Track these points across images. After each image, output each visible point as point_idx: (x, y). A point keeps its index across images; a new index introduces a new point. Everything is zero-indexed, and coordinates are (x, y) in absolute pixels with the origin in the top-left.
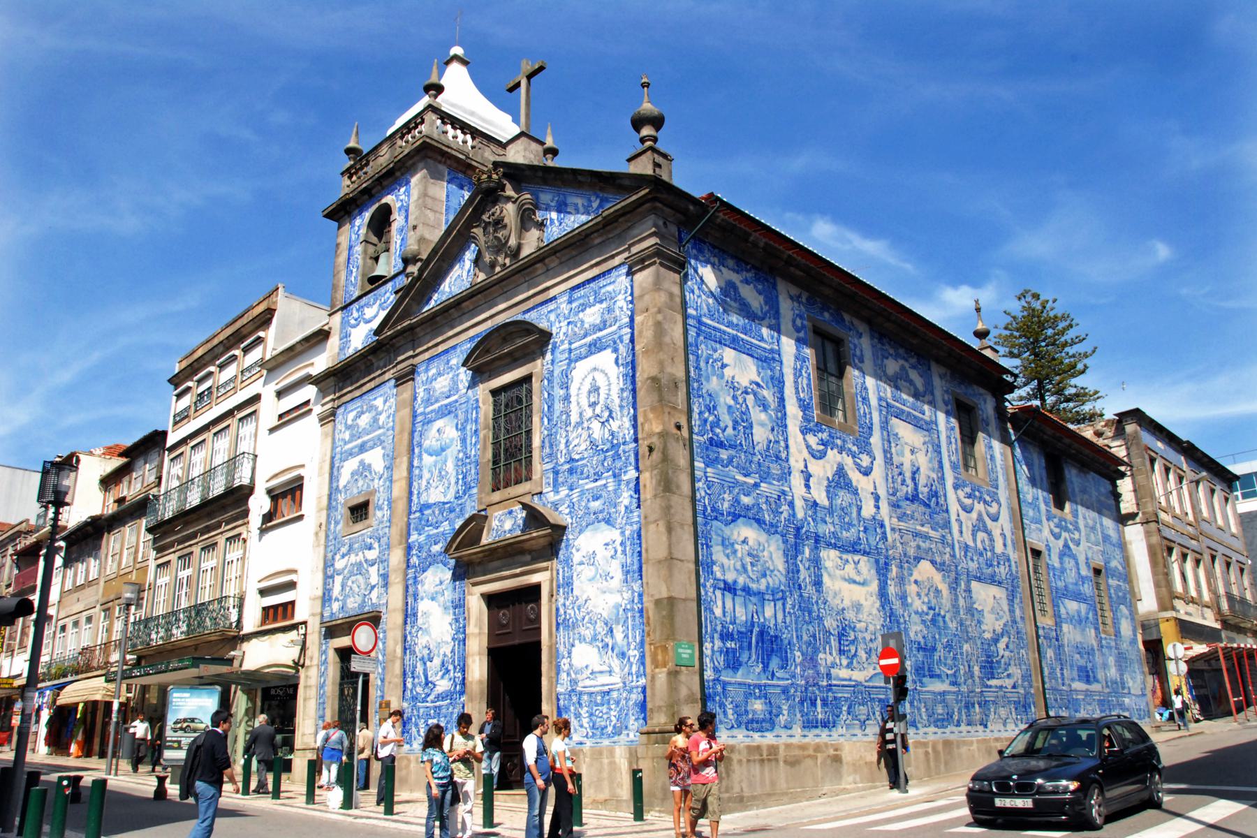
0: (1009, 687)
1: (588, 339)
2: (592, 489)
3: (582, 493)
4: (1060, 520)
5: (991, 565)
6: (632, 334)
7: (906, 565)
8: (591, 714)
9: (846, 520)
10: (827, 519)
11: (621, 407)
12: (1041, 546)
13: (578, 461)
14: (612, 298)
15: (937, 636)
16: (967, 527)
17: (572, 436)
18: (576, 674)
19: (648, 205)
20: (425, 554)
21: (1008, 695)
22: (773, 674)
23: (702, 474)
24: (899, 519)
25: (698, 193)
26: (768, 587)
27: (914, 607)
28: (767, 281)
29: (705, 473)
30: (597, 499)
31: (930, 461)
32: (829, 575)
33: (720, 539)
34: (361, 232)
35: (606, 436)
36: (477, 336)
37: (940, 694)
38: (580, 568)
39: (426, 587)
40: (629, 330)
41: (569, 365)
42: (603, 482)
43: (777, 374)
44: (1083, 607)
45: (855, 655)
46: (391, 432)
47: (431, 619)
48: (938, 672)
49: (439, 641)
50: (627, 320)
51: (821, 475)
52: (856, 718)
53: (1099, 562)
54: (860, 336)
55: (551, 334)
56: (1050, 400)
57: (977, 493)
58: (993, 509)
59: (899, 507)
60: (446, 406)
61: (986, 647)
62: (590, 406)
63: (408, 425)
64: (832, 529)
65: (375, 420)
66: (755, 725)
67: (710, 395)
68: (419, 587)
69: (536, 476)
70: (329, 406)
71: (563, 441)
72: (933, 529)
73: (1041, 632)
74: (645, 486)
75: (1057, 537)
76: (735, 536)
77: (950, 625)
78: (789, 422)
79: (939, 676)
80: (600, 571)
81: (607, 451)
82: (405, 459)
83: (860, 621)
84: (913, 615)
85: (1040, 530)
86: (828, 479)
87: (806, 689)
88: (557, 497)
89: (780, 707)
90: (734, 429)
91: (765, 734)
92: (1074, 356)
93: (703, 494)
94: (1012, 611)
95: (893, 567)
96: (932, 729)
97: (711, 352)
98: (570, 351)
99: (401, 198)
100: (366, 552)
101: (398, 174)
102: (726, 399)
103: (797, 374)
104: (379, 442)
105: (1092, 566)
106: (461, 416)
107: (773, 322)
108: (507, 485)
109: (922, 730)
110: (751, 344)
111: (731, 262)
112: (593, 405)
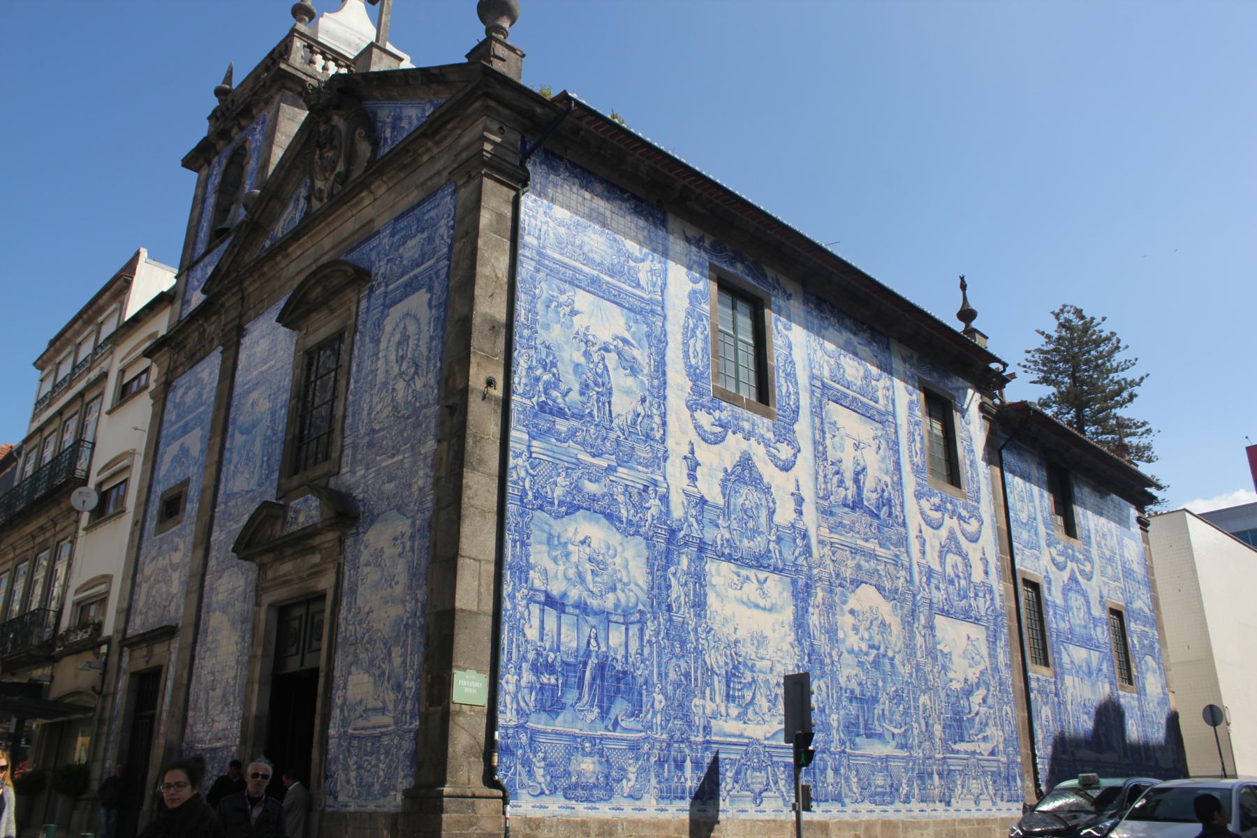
0: (985, 753)
1: (405, 278)
4: (1066, 548)
5: (966, 597)
6: (449, 266)
7: (838, 590)
8: (360, 767)
9: (751, 524)
10: (720, 522)
11: (429, 359)
12: (1037, 577)
13: (379, 431)
14: (435, 225)
15: (880, 684)
16: (932, 547)
17: (376, 399)
18: (349, 712)
19: (477, 104)
21: (985, 763)
22: (616, 724)
23: (524, 448)
24: (831, 530)
25: (552, 92)
26: (617, 606)
27: (848, 644)
28: (653, 216)
29: (529, 446)
31: (884, 458)
32: (718, 594)
33: (545, 536)
35: (410, 398)
37: (881, 759)
39: (220, 597)
41: (382, 312)
42: (401, 457)
43: (658, 331)
44: (1095, 656)
45: (751, 702)
48: (879, 730)
50: (445, 250)
51: (715, 465)
52: (747, 787)
53: (1118, 601)
54: (789, 297)
55: (370, 276)
56: (1090, 429)
57: (949, 506)
58: (972, 526)
59: (831, 514)
60: (262, 373)
61: (953, 700)
62: (397, 361)
64: (727, 536)
65: (200, 395)
66: (580, 792)
67: (548, 347)
69: (335, 455)
70: (163, 379)
71: (366, 407)
72: (881, 546)
73: (1033, 684)
75: (1061, 568)
76: (570, 534)
77: (901, 669)
78: (669, 392)
79: (880, 736)
82: (218, 440)
83: (762, 658)
84: (845, 654)
85: (1038, 558)
86: (726, 471)
87: (669, 746)
88: (353, 480)
89: (622, 769)
90: (582, 394)
91: (597, 805)
92: (1118, 382)
93: (523, 474)
94: (993, 656)
95: (819, 589)
96: (867, 805)
97: (555, 294)
98: (386, 294)
100: (172, 553)
101: (255, 111)
102: (571, 355)
103: (688, 333)
105: (1108, 605)
107: (658, 266)
109: (850, 807)
110: (620, 291)
111: (599, 188)
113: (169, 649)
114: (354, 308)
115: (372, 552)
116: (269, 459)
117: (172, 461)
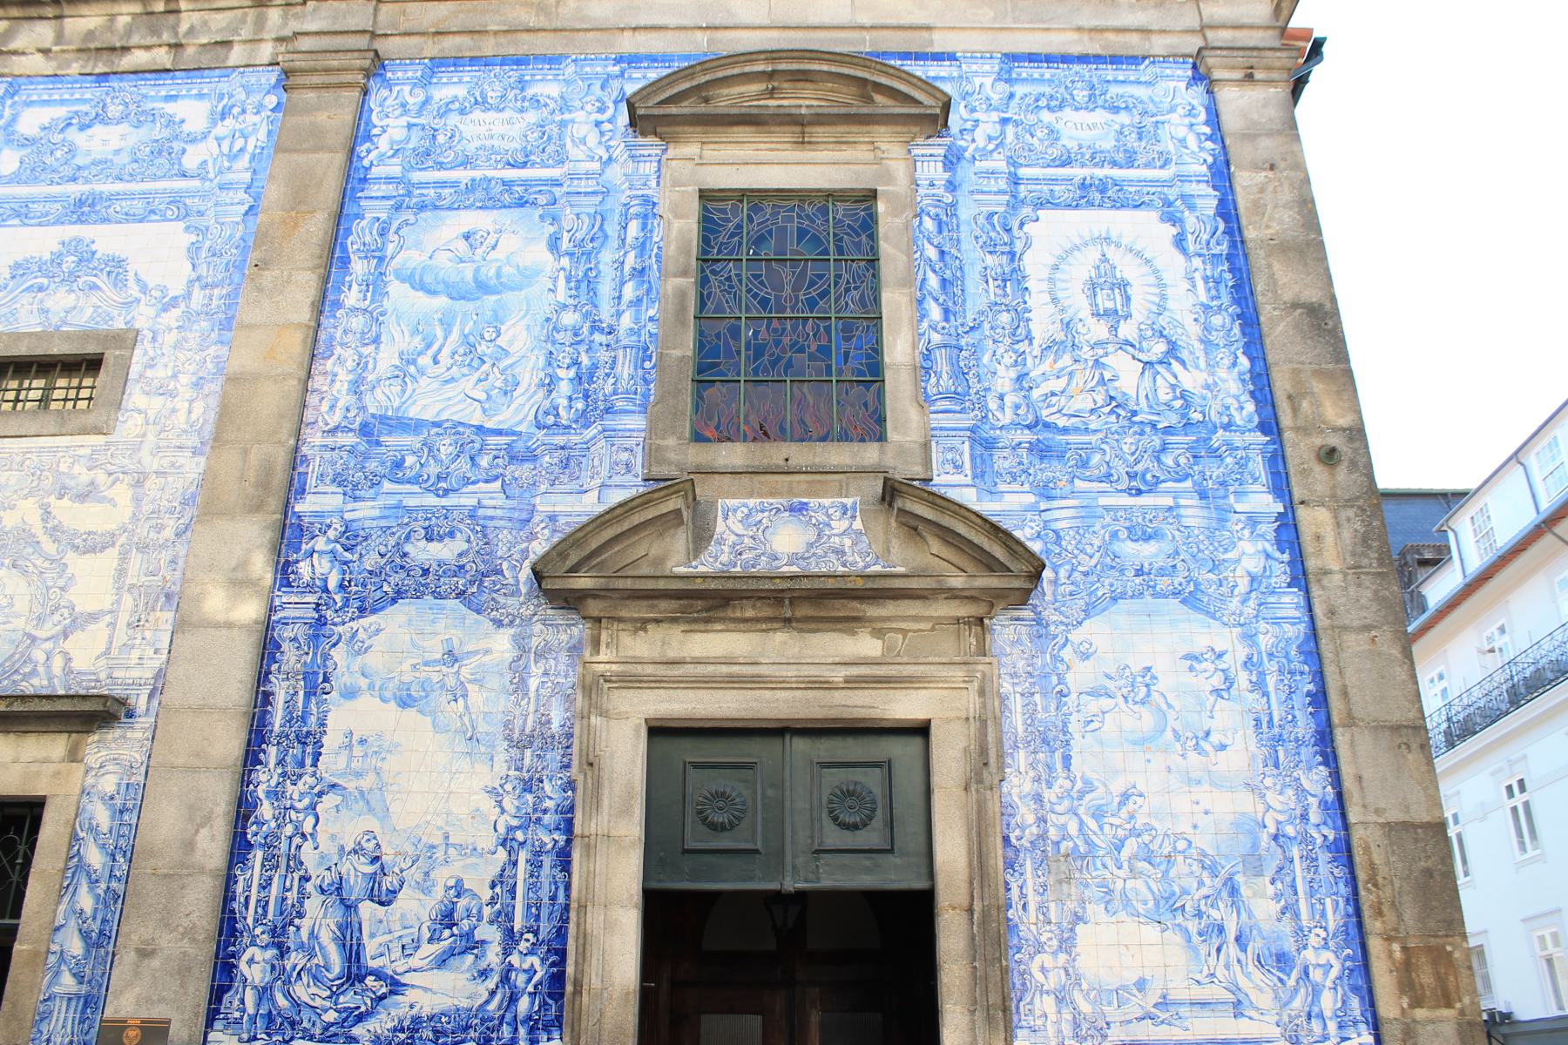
1: (1077, 172)
3: (1088, 514)
11: (1206, 343)
20: (371, 561)
30: (1147, 538)
35: (1164, 395)
36: (653, 59)
38: (1093, 705)
39: (373, 660)
40: (1210, 191)
42: (1169, 501)
46: (241, 195)
47: (391, 764)
49: (437, 839)
68: (338, 654)
74: (1318, 538)
80: (1171, 723)
81: (1168, 430)
104: (179, 208)
108: (782, 435)
112: (1113, 317)
113: (73, 756)
114: (899, 169)
115: (1112, 671)
117: (17, 265)
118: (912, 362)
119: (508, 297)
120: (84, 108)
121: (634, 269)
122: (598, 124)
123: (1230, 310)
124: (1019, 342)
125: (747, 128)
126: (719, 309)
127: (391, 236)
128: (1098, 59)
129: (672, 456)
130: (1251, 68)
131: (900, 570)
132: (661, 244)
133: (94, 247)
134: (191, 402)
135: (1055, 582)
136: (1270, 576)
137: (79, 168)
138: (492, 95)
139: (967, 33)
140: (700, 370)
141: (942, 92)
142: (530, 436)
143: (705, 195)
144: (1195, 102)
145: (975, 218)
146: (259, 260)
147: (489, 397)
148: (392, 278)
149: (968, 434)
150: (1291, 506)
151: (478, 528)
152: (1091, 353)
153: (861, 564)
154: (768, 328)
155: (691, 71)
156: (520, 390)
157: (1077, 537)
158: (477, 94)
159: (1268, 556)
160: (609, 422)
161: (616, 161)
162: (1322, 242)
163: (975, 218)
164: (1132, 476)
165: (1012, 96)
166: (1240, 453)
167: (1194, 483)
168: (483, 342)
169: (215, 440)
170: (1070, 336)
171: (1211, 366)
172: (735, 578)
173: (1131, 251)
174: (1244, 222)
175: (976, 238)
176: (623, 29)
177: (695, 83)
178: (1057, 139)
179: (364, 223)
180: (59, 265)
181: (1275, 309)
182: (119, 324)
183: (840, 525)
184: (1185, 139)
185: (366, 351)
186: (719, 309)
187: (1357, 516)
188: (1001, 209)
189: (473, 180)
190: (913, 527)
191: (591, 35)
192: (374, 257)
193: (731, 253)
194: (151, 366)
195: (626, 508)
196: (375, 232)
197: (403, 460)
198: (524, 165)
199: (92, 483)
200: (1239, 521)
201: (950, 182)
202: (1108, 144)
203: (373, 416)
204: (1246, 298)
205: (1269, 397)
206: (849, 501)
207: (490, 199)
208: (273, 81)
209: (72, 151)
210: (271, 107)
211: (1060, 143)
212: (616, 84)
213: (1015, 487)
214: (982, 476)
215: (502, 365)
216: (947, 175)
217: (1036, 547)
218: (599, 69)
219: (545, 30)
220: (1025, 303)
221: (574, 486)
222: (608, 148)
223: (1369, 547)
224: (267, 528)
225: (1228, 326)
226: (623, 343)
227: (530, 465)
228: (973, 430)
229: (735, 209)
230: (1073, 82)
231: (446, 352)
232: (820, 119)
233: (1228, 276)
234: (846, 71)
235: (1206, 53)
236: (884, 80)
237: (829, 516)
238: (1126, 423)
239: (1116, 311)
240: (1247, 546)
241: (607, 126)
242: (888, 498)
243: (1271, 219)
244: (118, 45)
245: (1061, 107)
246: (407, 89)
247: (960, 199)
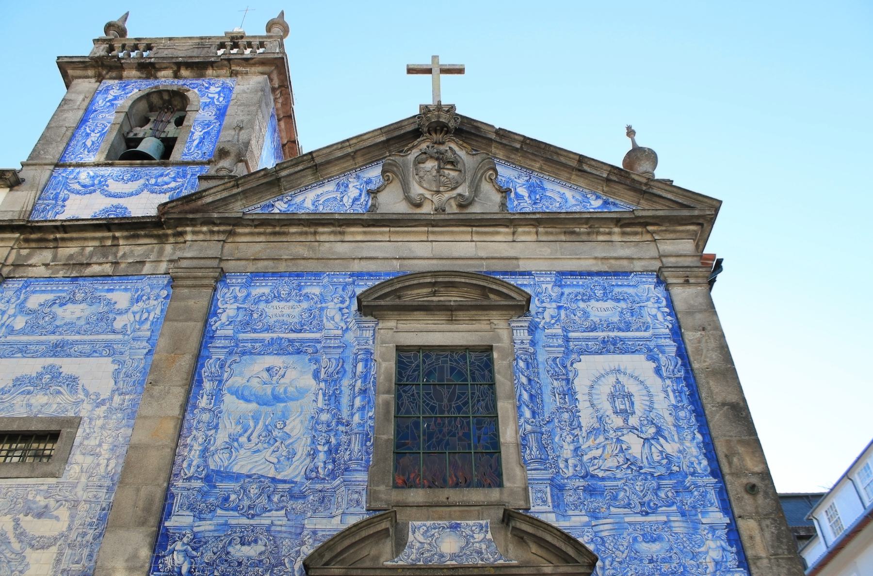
1: (601, 334)
2: (640, 523)
3: (619, 527)
20: (208, 557)
30: (654, 541)
34: (119, 103)
35: (656, 457)
36: (370, 274)
40: (672, 343)
42: (664, 518)
46: (145, 344)
60: (291, 341)
63: (193, 343)
81: (660, 477)
99: (210, 95)
104: (110, 350)
106: (328, 362)
108: (444, 485)
112: (625, 414)
114: (504, 334)
116: (330, 451)
117: (17, 379)
118: (515, 442)
119: (291, 404)
120: (64, 295)
121: (361, 389)
122: (341, 309)
123: (689, 408)
124: (574, 429)
125: (422, 313)
126: (408, 412)
127: (227, 369)
128: (606, 274)
129: (383, 496)
130: (688, 277)
131: (515, 562)
132: (376, 376)
133: (61, 370)
134: (108, 460)
135: (603, 568)
136: (726, 562)
137: (57, 327)
138: (284, 293)
139: (537, 261)
140: (398, 446)
141: (526, 293)
142: (302, 484)
143: (399, 349)
144: (659, 295)
145: (546, 361)
146: (152, 380)
147: (279, 461)
148: (226, 392)
149: (549, 482)
150: (733, 519)
151: (271, 538)
152: (614, 434)
153: (492, 560)
154: (435, 422)
155: (391, 282)
156: (296, 458)
157: (614, 541)
158: (276, 292)
159: (724, 549)
160: (347, 476)
161: (350, 329)
162: (735, 369)
163: (546, 361)
164: (642, 504)
165: (562, 294)
166: (702, 489)
167: (678, 507)
168: (276, 430)
169: (121, 482)
170: (602, 425)
171: (681, 440)
172: (420, 569)
173: (632, 377)
174: (692, 359)
175: (548, 371)
176: (354, 259)
177: (393, 288)
178: (588, 317)
179: (211, 361)
180: (41, 379)
181: (713, 406)
182: (71, 414)
183: (479, 536)
184: (656, 315)
185: (210, 433)
186: (408, 412)
187: (772, 524)
188: (561, 355)
189: (272, 339)
190: (521, 537)
191: (338, 261)
192: (216, 380)
193: (414, 380)
194: (87, 438)
195: (358, 527)
196: (217, 366)
197: (229, 497)
198: (300, 331)
199: (46, 507)
200: (705, 529)
201: (532, 341)
202: (616, 319)
203: (213, 470)
204: (696, 401)
205: (714, 456)
206: (483, 522)
207: (281, 349)
208: (166, 282)
209: (54, 318)
210: (164, 296)
211: (590, 318)
212: (350, 288)
213: (577, 512)
214: (558, 506)
215: (287, 443)
216: (530, 337)
217: (591, 547)
218: (341, 280)
219: (312, 259)
220: (577, 407)
221: (327, 513)
222: (346, 323)
223: (782, 542)
224: (148, 535)
225: (688, 416)
226: (356, 431)
227: (301, 501)
228: (552, 479)
229: (416, 357)
230: (594, 286)
231: (255, 435)
232: (461, 308)
233: (686, 389)
234: (474, 282)
235: (663, 270)
236: (494, 287)
237: (472, 531)
238: (637, 474)
239: (626, 411)
240: (711, 544)
241: (345, 311)
242: (506, 520)
243: (706, 357)
244: (85, 262)
245: (589, 300)
246: (238, 288)
247: (538, 350)
